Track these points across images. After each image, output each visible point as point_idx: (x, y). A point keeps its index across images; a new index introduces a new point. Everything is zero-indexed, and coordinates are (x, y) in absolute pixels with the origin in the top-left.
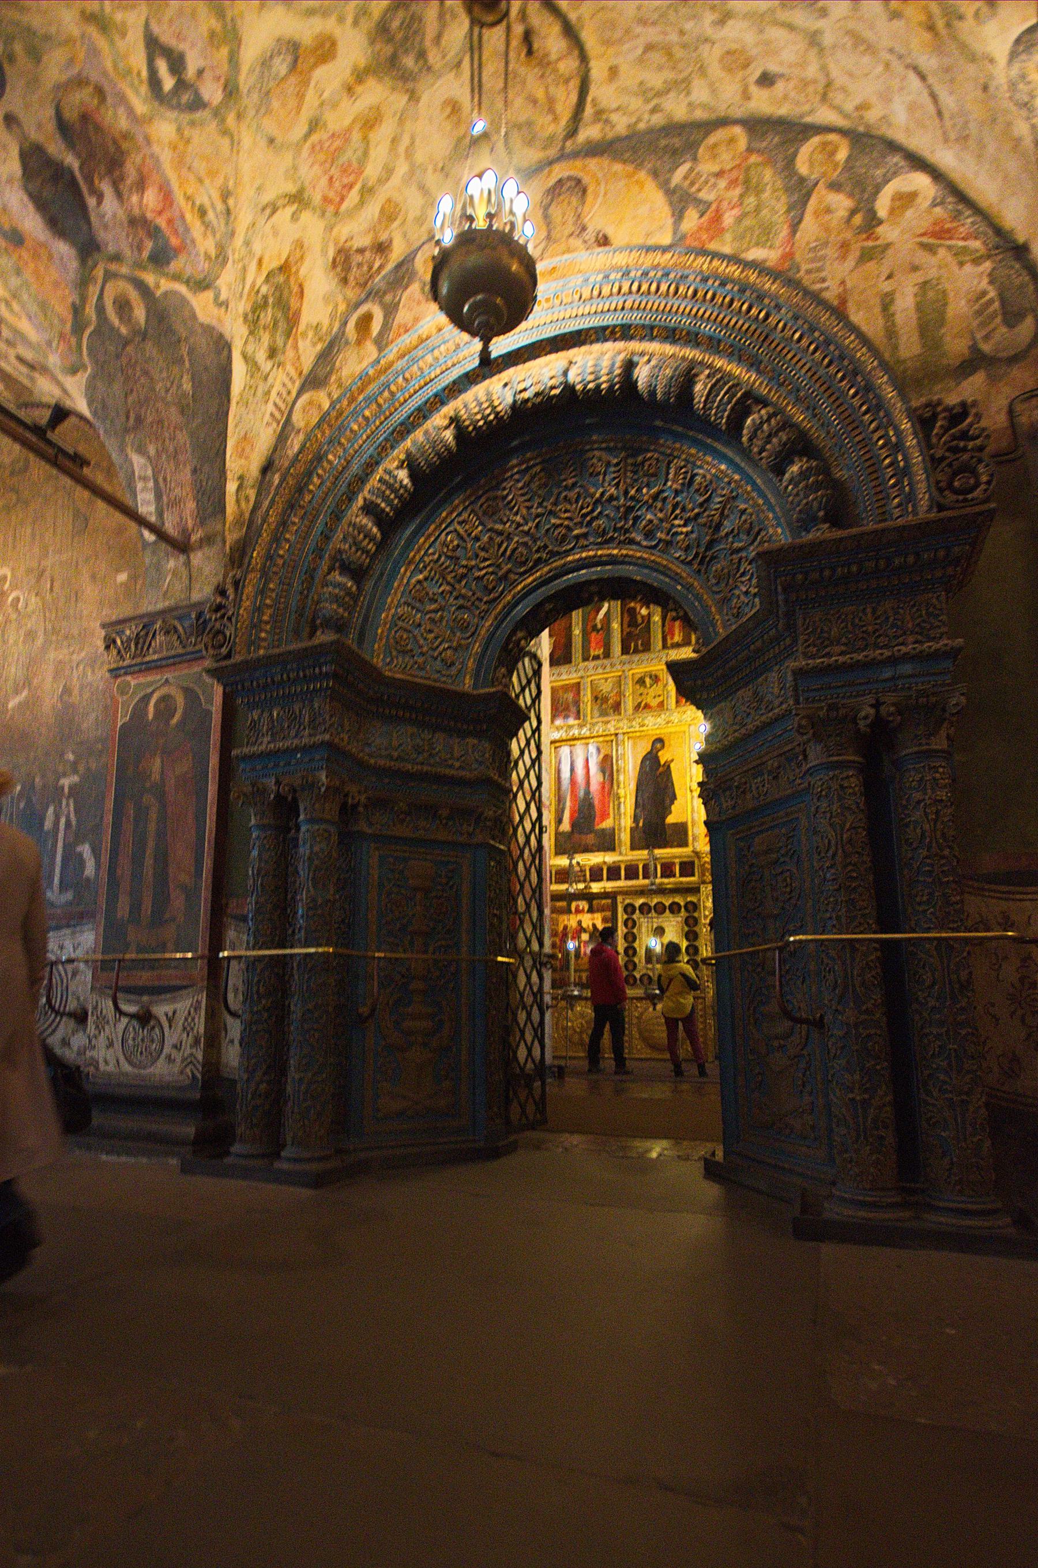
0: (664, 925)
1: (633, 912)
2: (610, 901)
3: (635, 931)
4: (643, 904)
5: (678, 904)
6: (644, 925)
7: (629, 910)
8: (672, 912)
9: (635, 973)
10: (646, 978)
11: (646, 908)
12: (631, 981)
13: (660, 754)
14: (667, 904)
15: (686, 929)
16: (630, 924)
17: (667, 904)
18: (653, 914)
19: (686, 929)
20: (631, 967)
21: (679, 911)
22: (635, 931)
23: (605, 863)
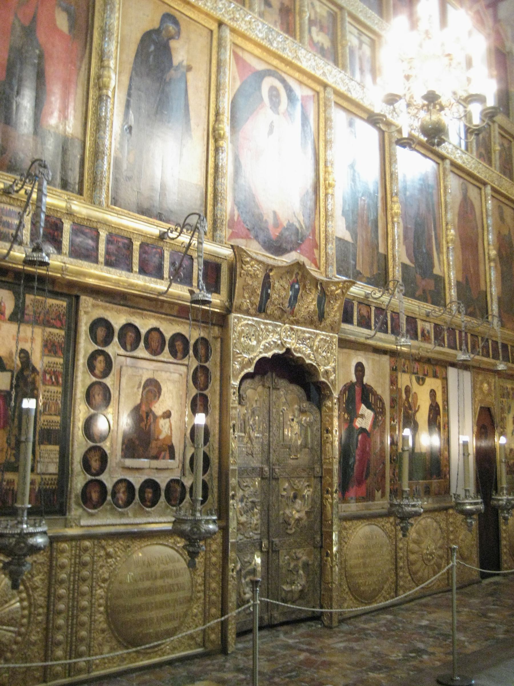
0: (162, 377)
1: (107, 341)
2: (63, 303)
3: (108, 381)
4: (129, 326)
5: (185, 340)
6: (127, 372)
7: (101, 332)
8: (174, 353)
9: (103, 478)
10: (122, 488)
11: (131, 335)
12: (95, 496)
13: (173, 44)
14: (168, 336)
15: (194, 391)
16: (100, 364)
17: (168, 336)
18: (141, 352)
19: (194, 391)
20: (95, 464)
21: (185, 353)
22: (108, 381)
23: (70, 214)
